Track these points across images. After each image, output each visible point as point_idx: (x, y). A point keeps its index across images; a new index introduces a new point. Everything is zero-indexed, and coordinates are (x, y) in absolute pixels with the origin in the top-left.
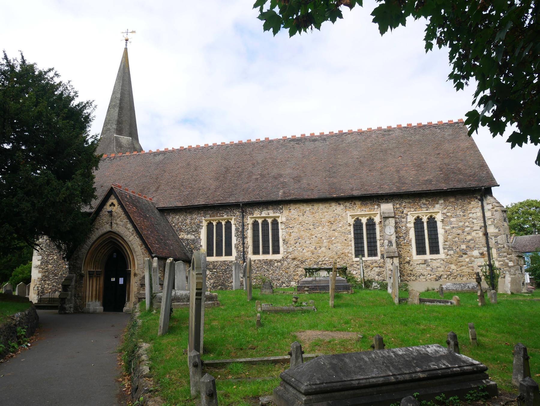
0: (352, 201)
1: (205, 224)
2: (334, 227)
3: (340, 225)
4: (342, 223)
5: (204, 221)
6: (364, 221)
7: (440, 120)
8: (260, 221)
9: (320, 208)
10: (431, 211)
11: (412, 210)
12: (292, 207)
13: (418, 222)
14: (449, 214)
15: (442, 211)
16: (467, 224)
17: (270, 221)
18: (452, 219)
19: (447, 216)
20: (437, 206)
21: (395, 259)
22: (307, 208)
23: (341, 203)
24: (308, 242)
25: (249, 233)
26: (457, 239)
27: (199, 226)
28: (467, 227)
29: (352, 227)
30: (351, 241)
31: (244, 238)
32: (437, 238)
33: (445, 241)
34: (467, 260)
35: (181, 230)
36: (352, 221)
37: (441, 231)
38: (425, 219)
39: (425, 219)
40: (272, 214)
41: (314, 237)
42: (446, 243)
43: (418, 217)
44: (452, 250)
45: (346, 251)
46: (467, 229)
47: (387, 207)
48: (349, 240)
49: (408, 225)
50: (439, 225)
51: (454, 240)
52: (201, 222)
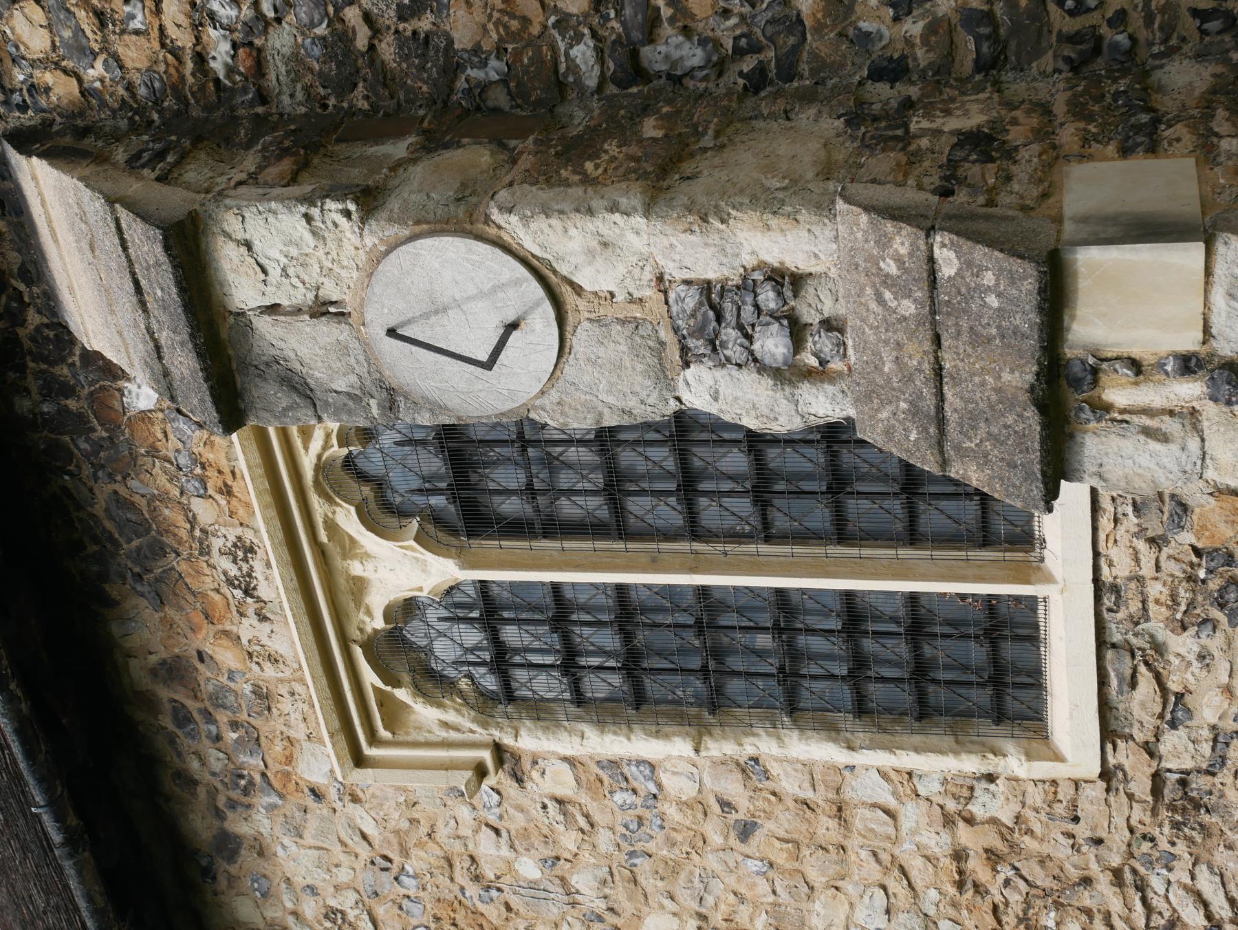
0: (149, 702)
3: (529, 869)
4: (487, 848)
6: (399, 570)
21: (1091, 328)
23: (200, 827)
29: (528, 740)
30: (752, 768)
45: (938, 842)
48: (733, 787)
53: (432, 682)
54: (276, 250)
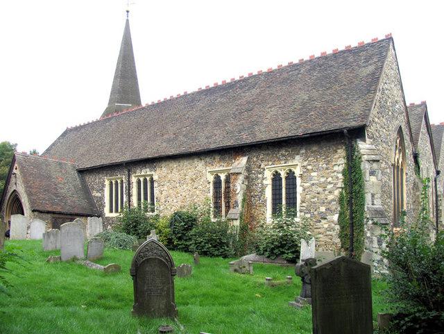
0: (212, 156)
1: (107, 183)
2: (196, 185)
4: (202, 180)
5: (106, 180)
7: (347, 45)
8: (142, 179)
9: (185, 163)
10: (290, 164)
11: (270, 163)
12: (163, 164)
13: (276, 178)
14: (309, 167)
15: (302, 163)
16: (330, 179)
17: (148, 178)
18: (313, 174)
19: (308, 170)
20: (297, 157)
22: (174, 165)
24: (175, 201)
25: (134, 191)
26: (316, 199)
27: (104, 186)
28: (330, 183)
31: (129, 196)
32: (295, 198)
33: (303, 202)
34: (326, 226)
35: (93, 189)
36: (211, 178)
37: (299, 190)
38: (283, 175)
39: (283, 175)
40: (148, 173)
41: (179, 195)
42: (304, 204)
43: (276, 172)
44: (310, 213)
46: (329, 187)
47: (243, 161)
49: (265, 182)
50: (299, 181)
51: (313, 200)
52: (104, 181)
53: (215, 178)
54: (241, 178)
